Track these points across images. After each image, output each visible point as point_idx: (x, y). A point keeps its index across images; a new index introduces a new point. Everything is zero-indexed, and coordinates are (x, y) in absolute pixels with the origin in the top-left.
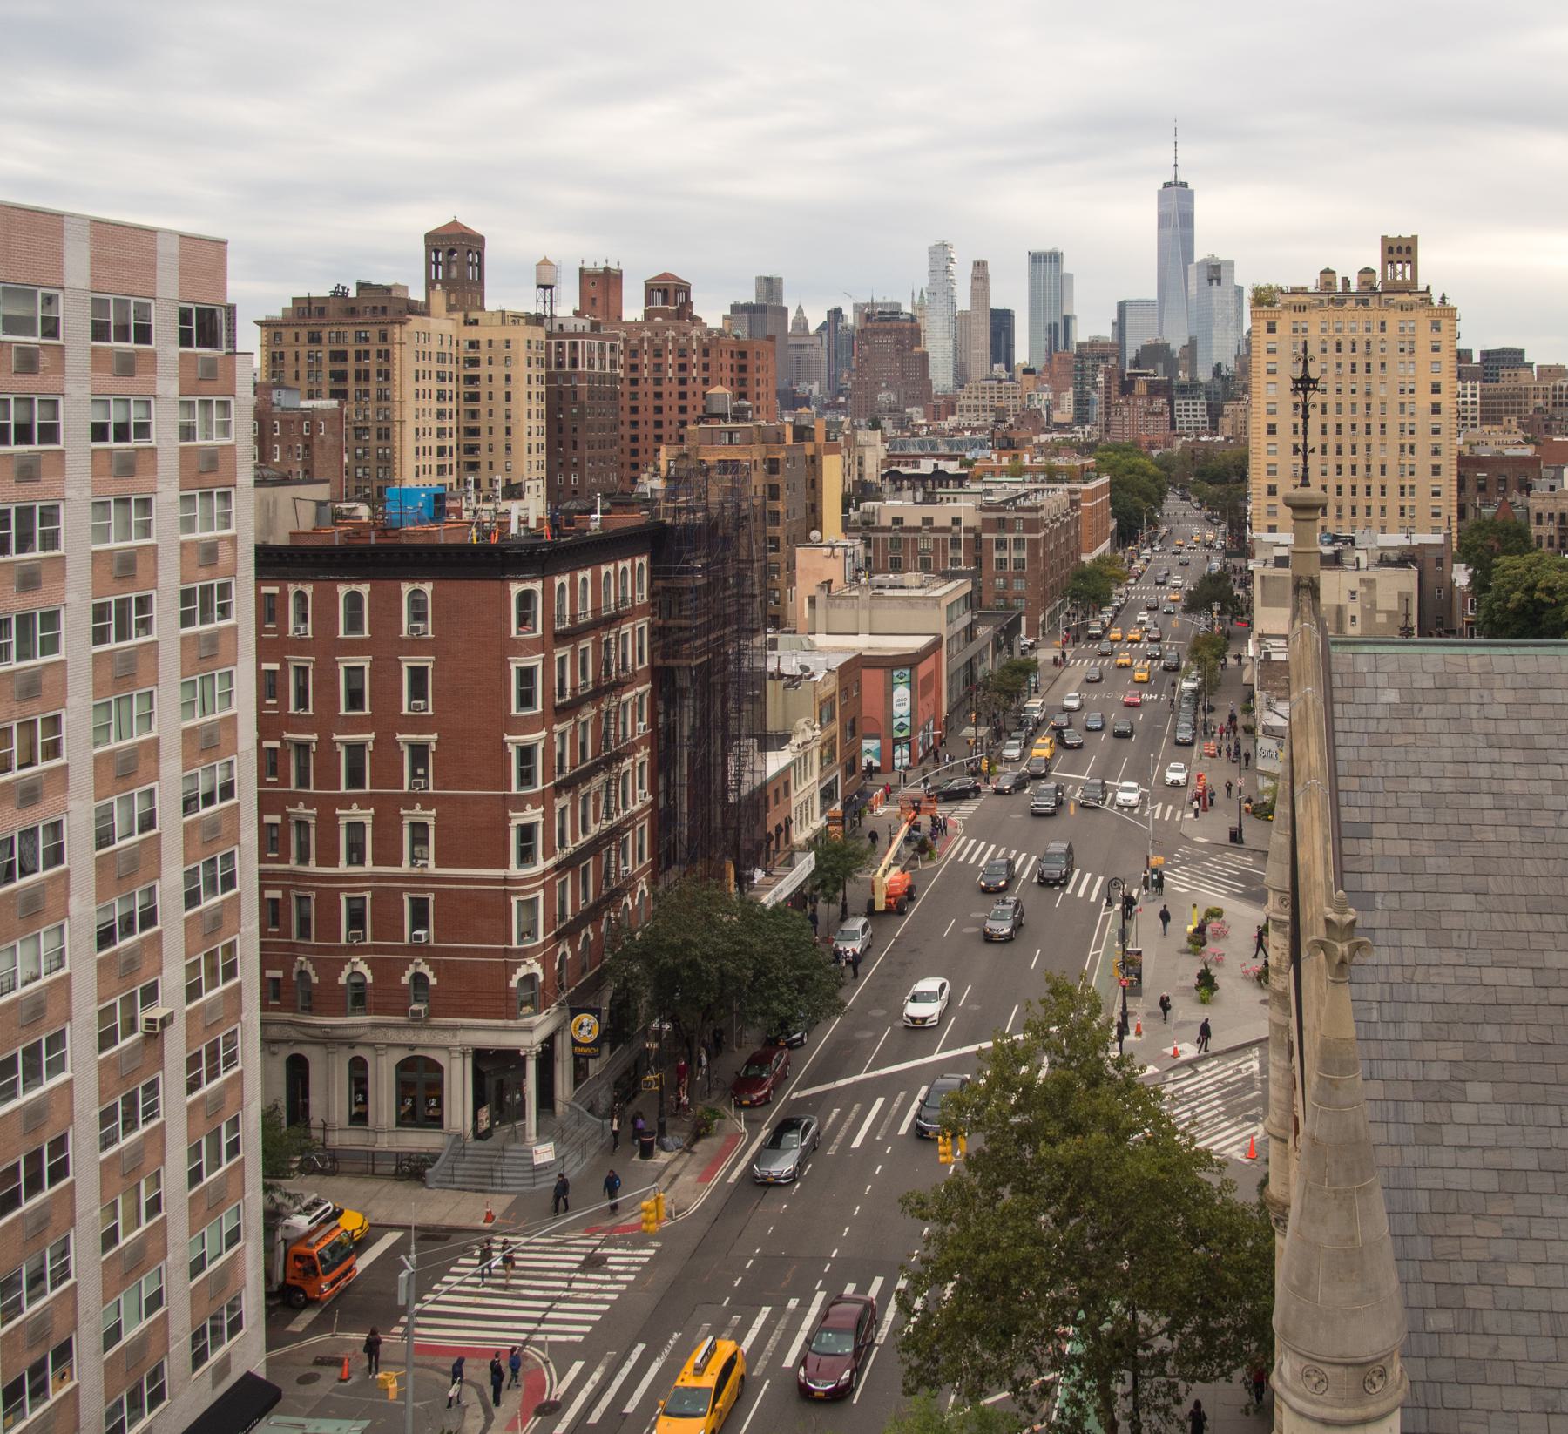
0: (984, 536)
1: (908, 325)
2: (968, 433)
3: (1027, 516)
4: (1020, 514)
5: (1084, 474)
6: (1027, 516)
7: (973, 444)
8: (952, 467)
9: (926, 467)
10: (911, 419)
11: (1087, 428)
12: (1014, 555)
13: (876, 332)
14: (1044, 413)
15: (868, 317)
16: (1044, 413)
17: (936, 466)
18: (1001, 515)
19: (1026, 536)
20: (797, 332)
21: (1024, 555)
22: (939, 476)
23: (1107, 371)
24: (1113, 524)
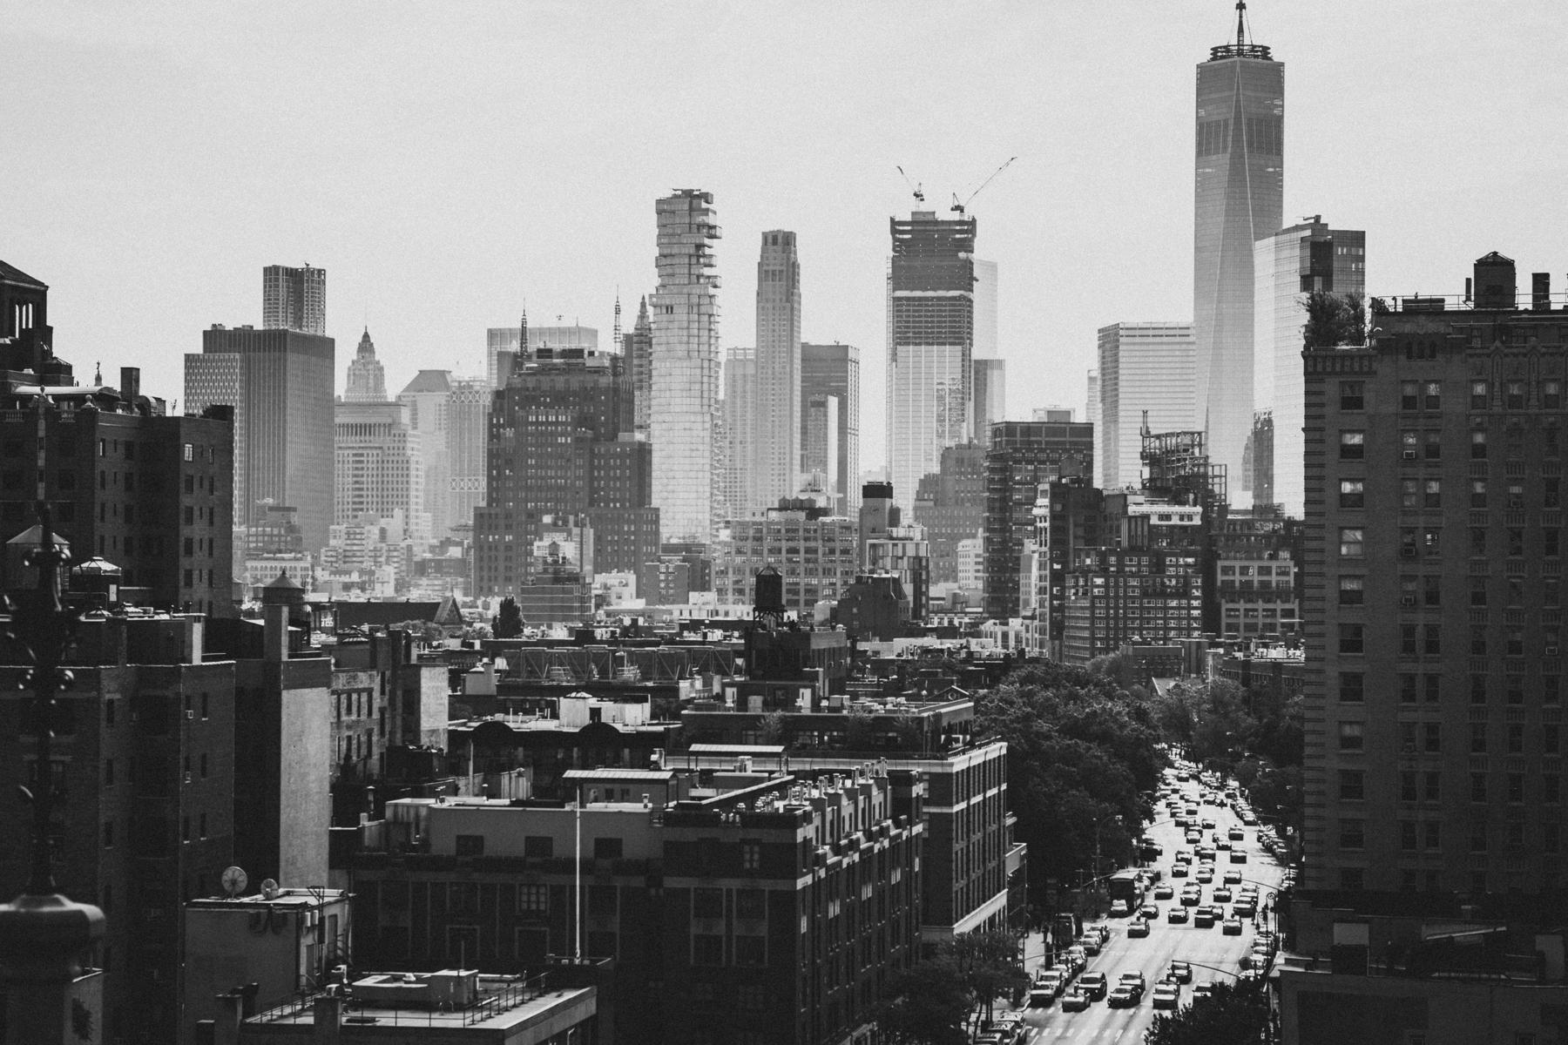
0: (672, 882)
1: (605, 381)
2: (717, 635)
3: (770, 836)
4: (754, 834)
5: (933, 740)
6: (770, 836)
7: (711, 662)
8: (633, 717)
9: (573, 713)
10: (602, 601)
11: (1015, 624)
12: (738, 929)
13: (530, 398)
14: (908, 589)
15: (518, 359)
16: (908, 589)
17: (595, 713)
18: (706, 833)
19: (767, 885)
20: (362, 396)
21: (763, 930)
22: (599, 741)
23: (1057, 492)
24: (1014, 856)
